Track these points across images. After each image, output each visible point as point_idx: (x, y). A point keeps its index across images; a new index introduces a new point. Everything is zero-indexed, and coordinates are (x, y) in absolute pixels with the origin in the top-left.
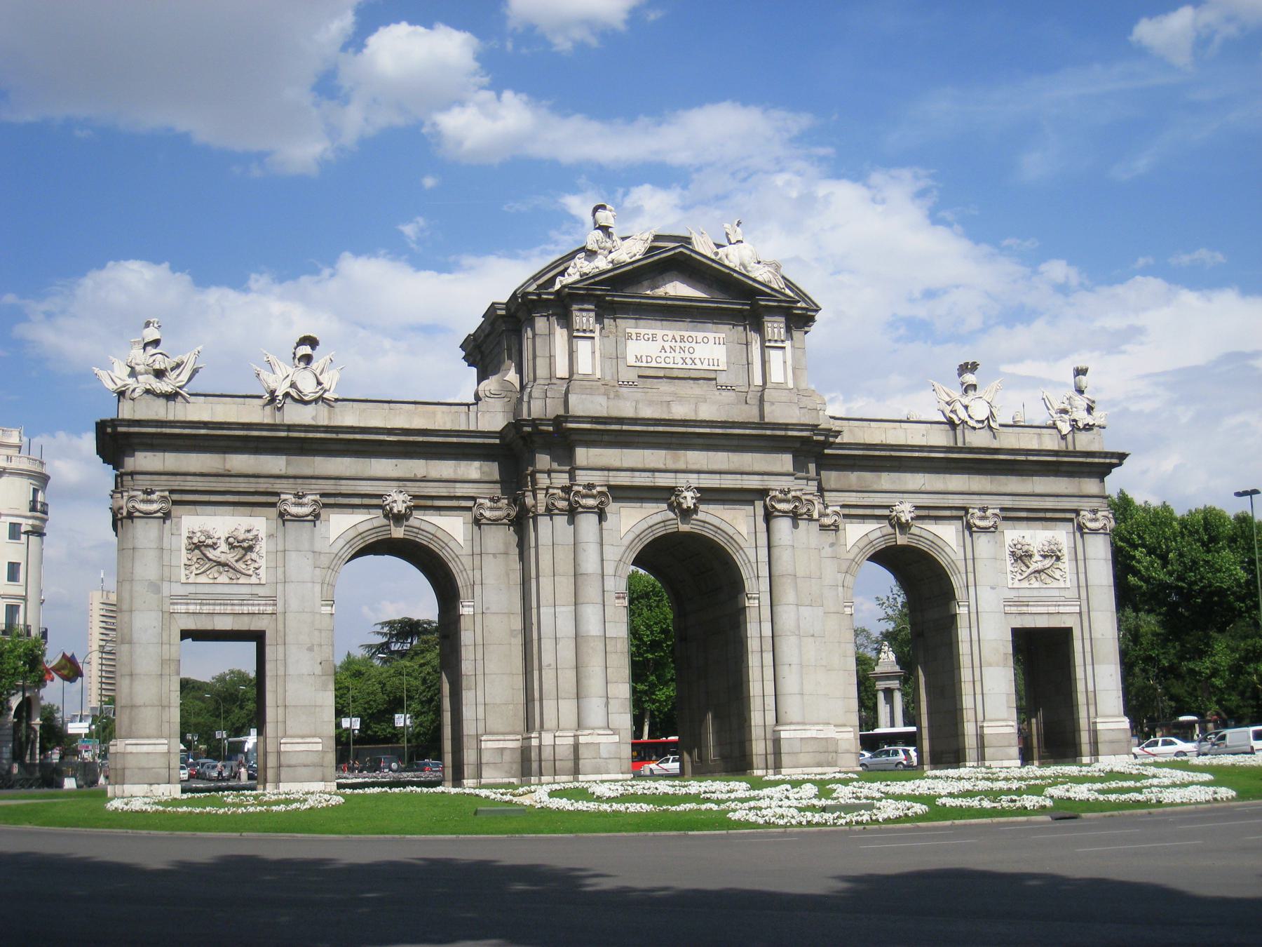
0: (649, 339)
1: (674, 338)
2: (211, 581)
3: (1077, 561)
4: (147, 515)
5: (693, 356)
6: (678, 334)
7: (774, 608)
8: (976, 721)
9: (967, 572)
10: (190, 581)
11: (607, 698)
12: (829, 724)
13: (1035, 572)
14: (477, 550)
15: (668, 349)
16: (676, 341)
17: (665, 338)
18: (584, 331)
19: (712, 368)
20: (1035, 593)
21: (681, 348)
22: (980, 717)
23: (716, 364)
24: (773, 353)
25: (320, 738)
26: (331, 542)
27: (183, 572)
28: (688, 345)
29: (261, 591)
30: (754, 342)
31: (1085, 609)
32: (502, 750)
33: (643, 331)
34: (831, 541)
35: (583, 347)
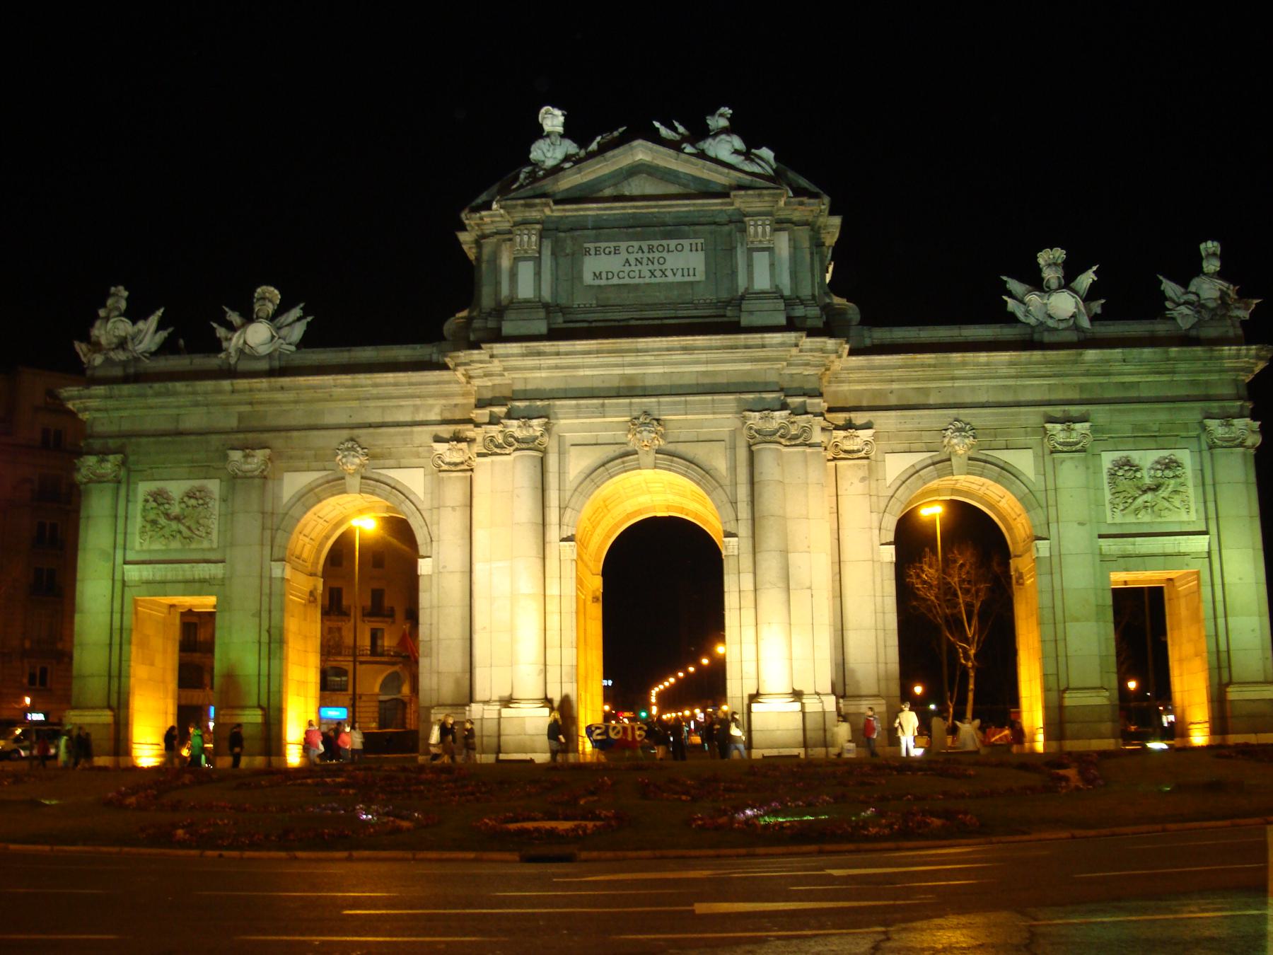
0: (610, 252)
1: (640, 248)
2: (164, 548)
3: (1203, 485)
4: (100, 480)
5: (663, 267)
6: (645, 245)
8: (1059, 690)
10: (145, 547)
11: (545, 665)
13: (1146, 502)
16: (643, 252)
17: (630, 250)
19: (686, 279)
21: (649, 259)
23: (691, 273)
24: (755, 254)
27: (138, 539)
28: (657, 255)
29: (212, 556)
30: (739, 245)
31: (1215, 548)
33: (603, 245)
35: (526, 271)
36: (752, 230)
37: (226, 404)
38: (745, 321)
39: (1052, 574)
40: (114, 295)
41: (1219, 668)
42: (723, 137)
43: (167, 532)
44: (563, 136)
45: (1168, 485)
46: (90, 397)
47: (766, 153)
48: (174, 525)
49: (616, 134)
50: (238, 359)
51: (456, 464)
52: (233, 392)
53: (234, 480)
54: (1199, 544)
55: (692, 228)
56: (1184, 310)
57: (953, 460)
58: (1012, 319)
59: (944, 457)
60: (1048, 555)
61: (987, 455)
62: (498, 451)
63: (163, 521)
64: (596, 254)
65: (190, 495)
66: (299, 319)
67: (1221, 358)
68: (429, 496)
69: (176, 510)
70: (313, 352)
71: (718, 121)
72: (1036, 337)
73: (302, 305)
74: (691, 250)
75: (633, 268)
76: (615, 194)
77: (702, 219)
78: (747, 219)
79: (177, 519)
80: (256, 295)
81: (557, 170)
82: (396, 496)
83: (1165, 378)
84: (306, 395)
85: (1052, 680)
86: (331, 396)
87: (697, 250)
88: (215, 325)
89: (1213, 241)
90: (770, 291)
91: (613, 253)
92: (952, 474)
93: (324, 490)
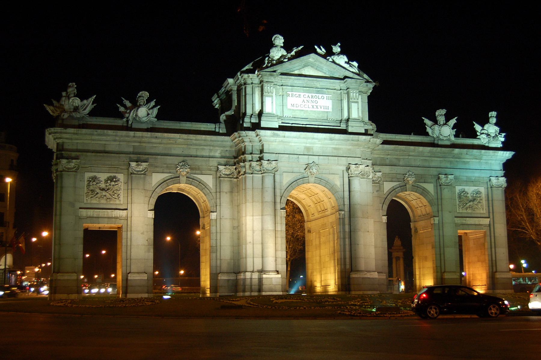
1: (308, 96)
2: (98, 202)
5: (317, 105)
6: (310, 95)
7: (351, 219)
8: (441, 272)
9: (438, 205)
11: (276, 258)
12: (375, 271)
13: (470, 205)
14: (218, 190)
15: (306, 101)
16: (309, 98)
18: (268, 93)
19: (325, 110)
20: (469, 215)
22: (443, 271)
23: (327, 108)
25: (146, 273)
26: (153, 186)
28: (315, 99)
30: (344, 100)
31: (492, 223)
32: (228, 280)
33: (295, 93)
34: (377, 189)
36: (352, 94)
37: (129, 142)
38: (350, 130)
39: (439, 230)
40: (70, 86)
41: (492, 266)
42: (342, 56)
43: (99, 195)
44: (281, 47)
45: (477, 200)
46: (66, 133)
47: (355, 64)
48: (104, 193)
49: (300, 48)
50: (132, 123)
51: (226, 175)
52: (134, 137)
53: (130, 175)
54: (486, 221)
55: (327, 90)
56: (484, 136)
57: (407, 186)
58: (427, 134)
59: (404, 184)
60: (438, 223)
61: (418, 185)
62: (256, 172)
63: (98, 191)
64: (292, 97)
65: (111, 179)
66: (154, 107)
67: (497, 156)
68: (215, 187)
69: (103, 185)
70: (164, 122)
71: (336, 49)
72: (436, 142)
73: (155, 100)
74: (327, 99)
75: (306, 104)
76: (299, 73)
77: (331, 87)
78: (350, 90)
79: (103, 190)
80: (139, 95)
81: (280, 62)
82: (201, 186)
83: (477, 161)
84: (164, 141)
85: (439, 268)
86: (176, 142)
87: (329, 99)
88: (119, 106)
89: (495, 111)
90: (357, 119)
91: (298, 96)
92: (406, 191)
93: (171, 181)
